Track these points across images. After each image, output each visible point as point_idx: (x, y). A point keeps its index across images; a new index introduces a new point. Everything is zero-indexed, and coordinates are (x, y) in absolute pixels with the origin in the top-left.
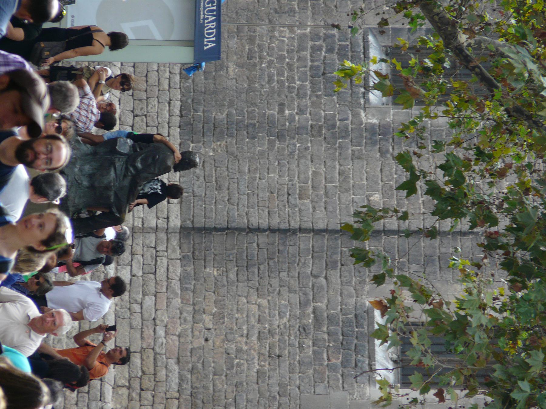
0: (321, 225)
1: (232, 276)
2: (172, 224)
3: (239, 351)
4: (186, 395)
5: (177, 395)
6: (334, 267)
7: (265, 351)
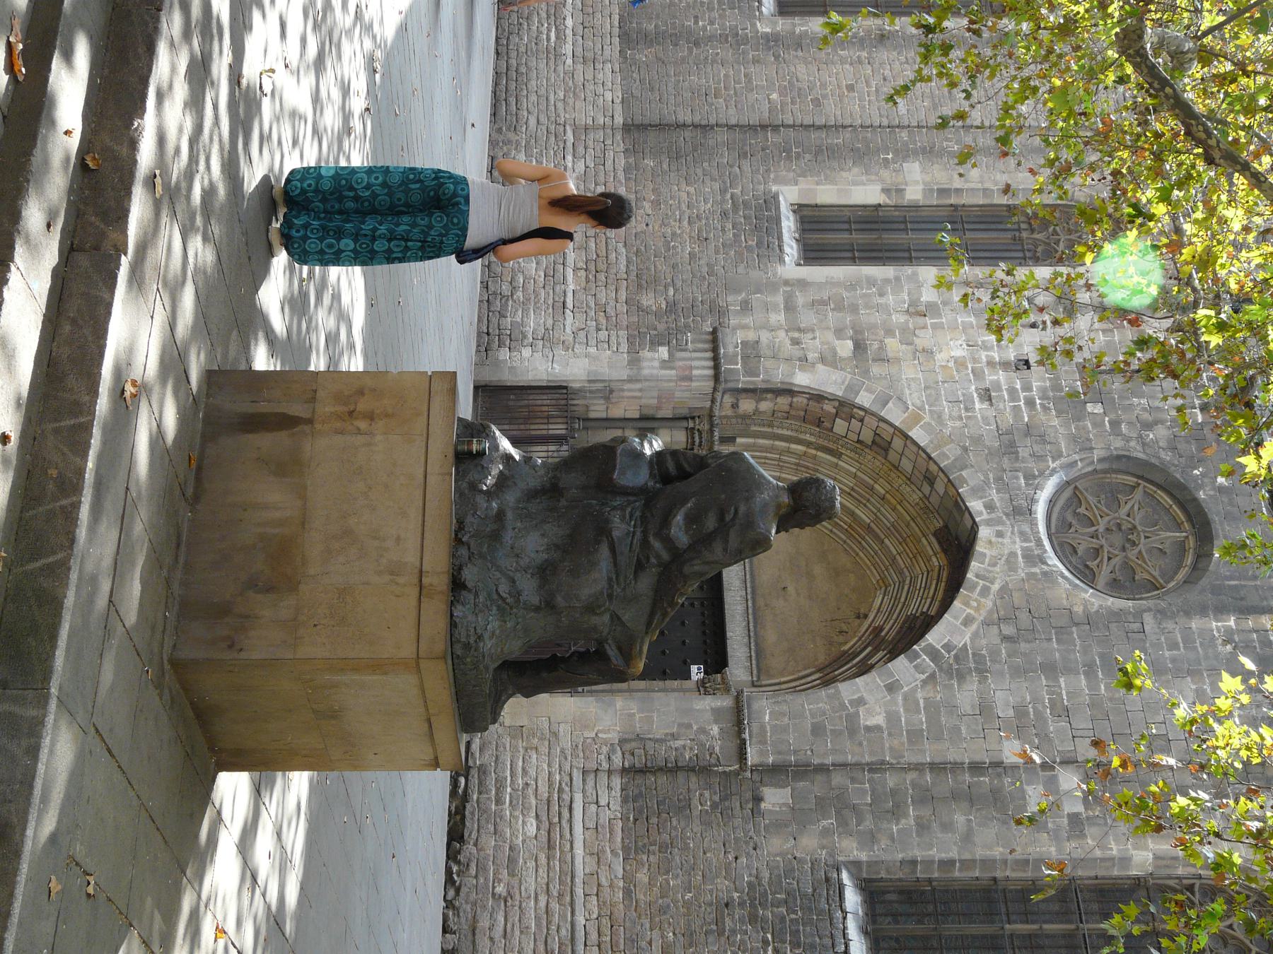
0: (733, 121)
1: (665, 166)
2: (616, 121)
3: (674, 234)
4: (633, 276)
5: (625, 276)
6: (746, 157)
7: (695, 234)
